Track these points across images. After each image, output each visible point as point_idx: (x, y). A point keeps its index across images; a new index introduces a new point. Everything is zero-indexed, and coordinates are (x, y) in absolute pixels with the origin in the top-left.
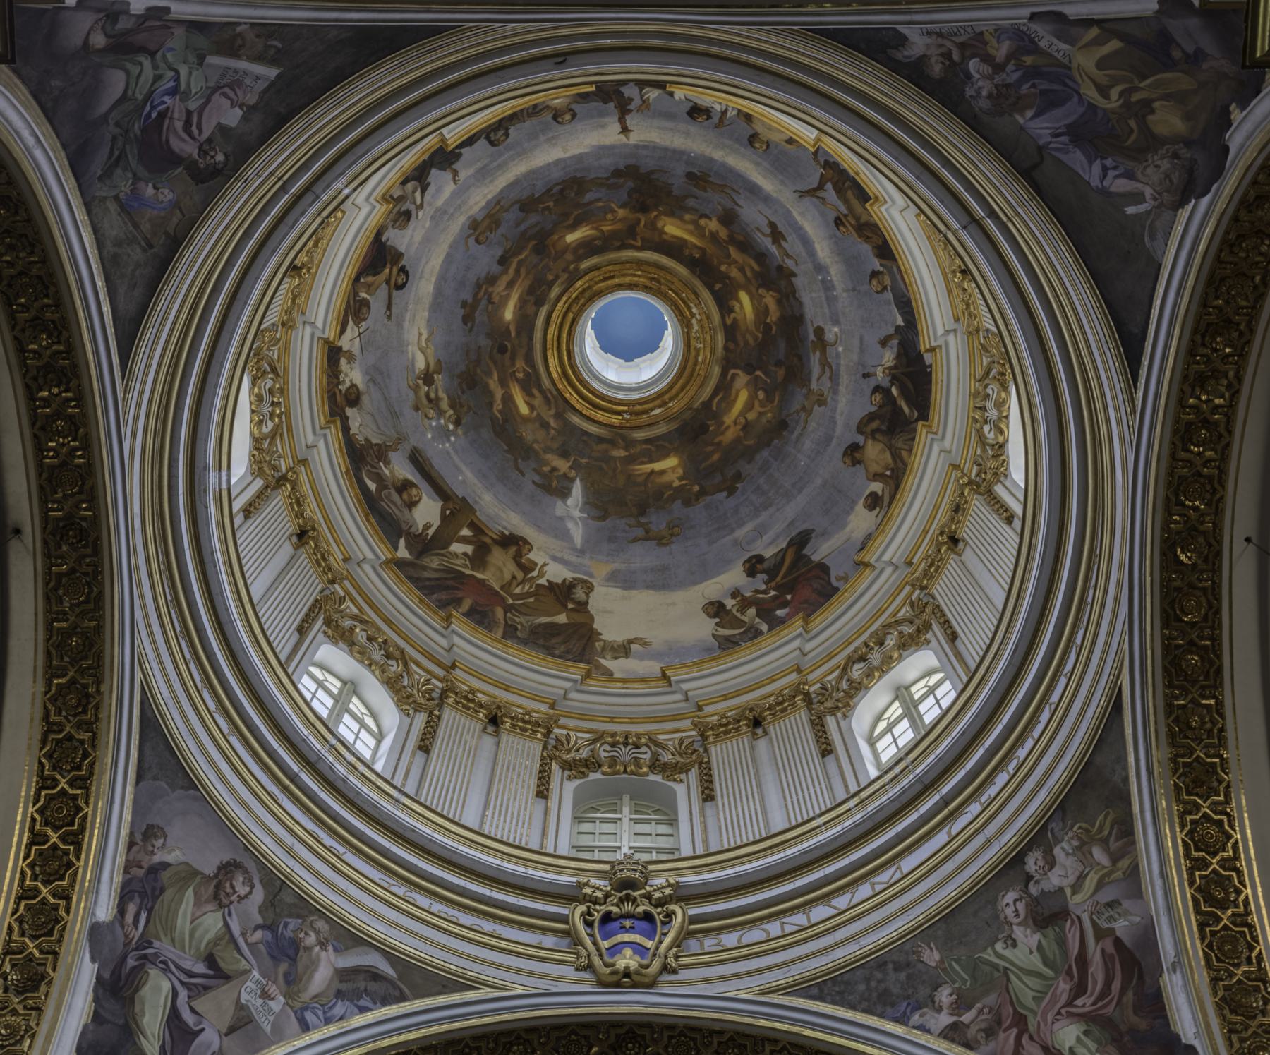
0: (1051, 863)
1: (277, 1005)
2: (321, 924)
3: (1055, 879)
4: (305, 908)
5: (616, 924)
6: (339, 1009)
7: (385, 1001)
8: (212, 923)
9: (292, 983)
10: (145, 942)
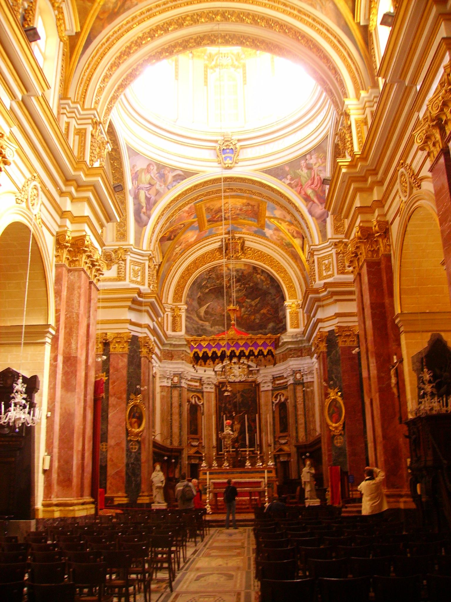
0: (311, 158)
1: (163, 187)
2: (168, 169)
3: (313, 161)
4: (164, 167)
5: (225, 151)
6: (174, 184)
7: (183, 180)
8: (148, 177)
9: (165, 182)
10: (138, 186)
